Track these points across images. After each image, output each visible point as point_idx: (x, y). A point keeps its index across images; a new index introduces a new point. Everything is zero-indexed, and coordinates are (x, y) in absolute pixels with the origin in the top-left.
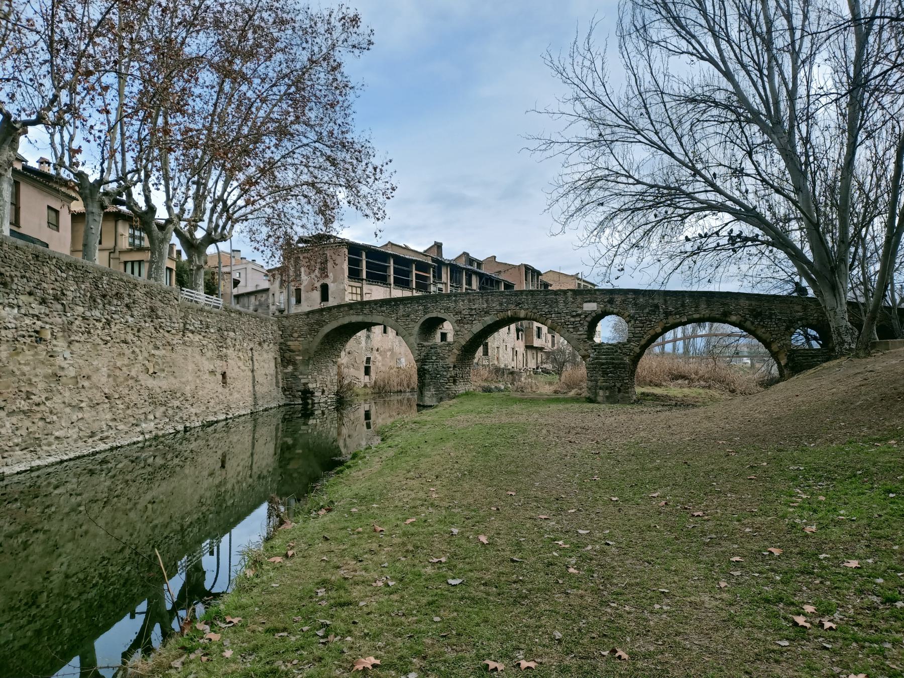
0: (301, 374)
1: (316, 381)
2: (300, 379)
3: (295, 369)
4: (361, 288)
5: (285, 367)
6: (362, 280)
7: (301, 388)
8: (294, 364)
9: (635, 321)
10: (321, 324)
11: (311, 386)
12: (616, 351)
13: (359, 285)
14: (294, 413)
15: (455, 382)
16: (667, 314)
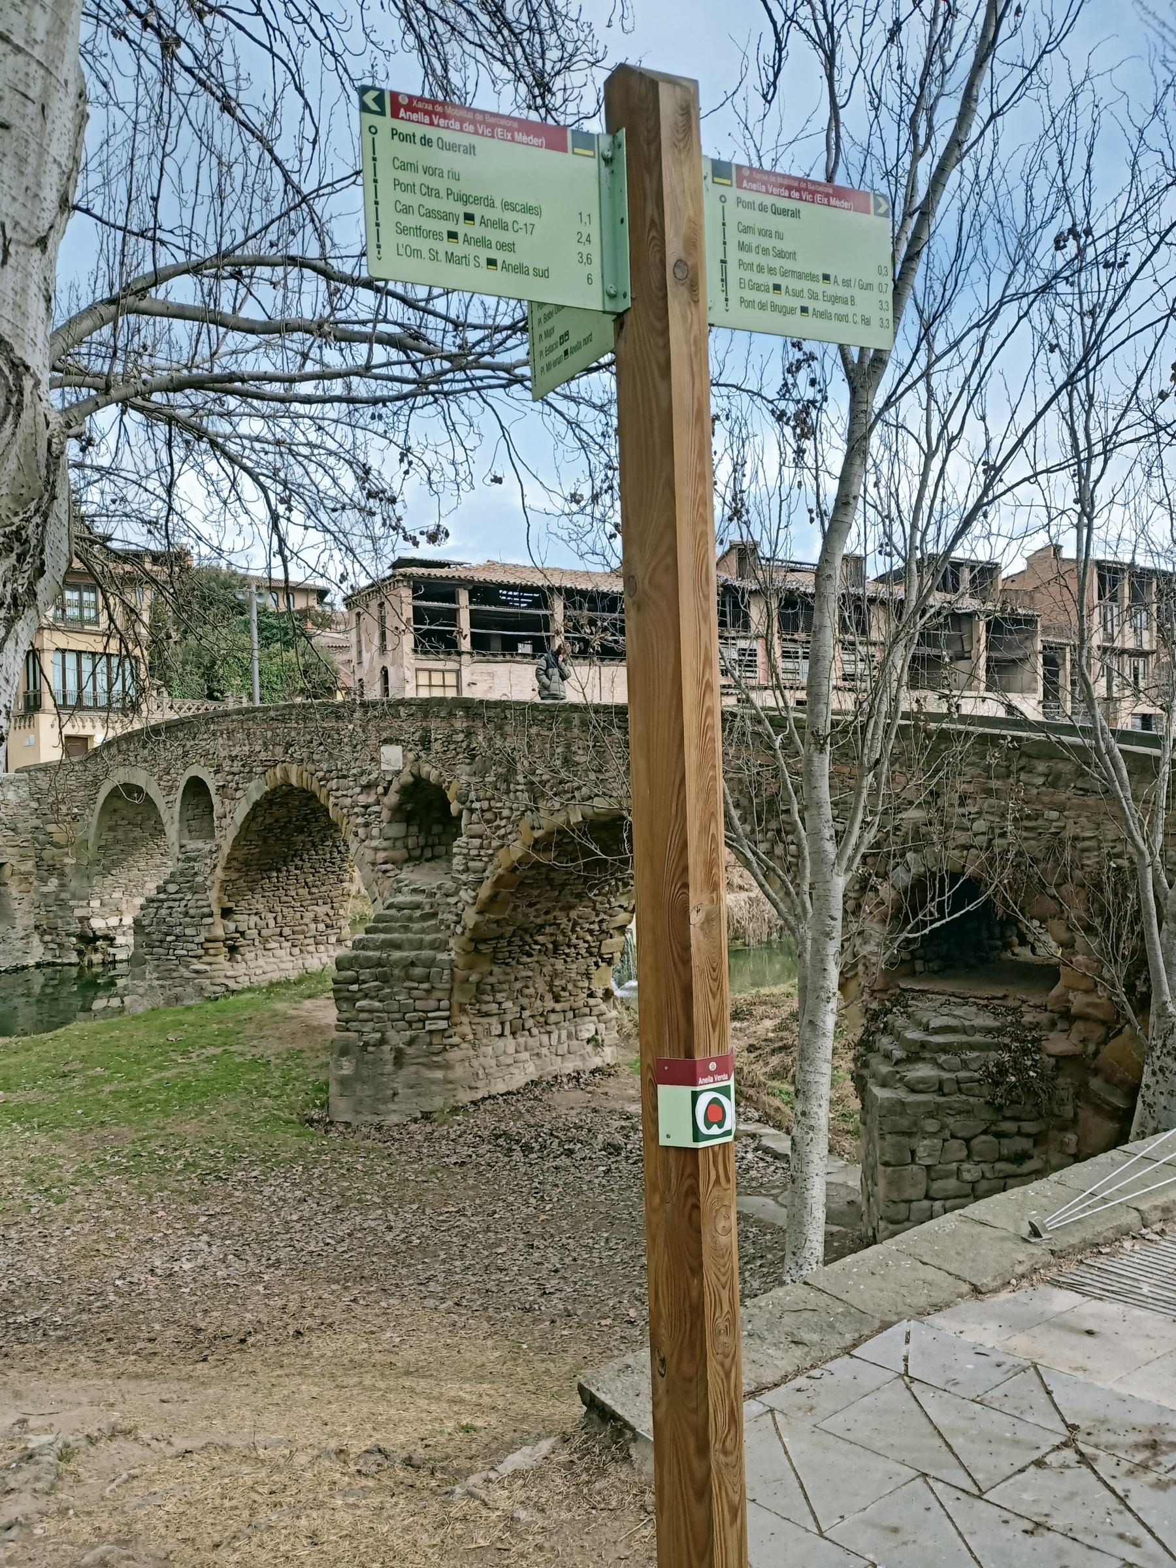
0: (74, 896)
1: (119, 912)
2: (72, 909)
3: (62, 886)
4: (458, 672)
5: (44, 881)
6: (459, 654)
7: (75, 927)
8: (62, 875)
9: (472, 811)
10: (96, 783)
11: (97, 924)
12: (434, 915)
13: (451, 665)
14: (62, 982)
15: (233, 950)
16: (535, 792)
